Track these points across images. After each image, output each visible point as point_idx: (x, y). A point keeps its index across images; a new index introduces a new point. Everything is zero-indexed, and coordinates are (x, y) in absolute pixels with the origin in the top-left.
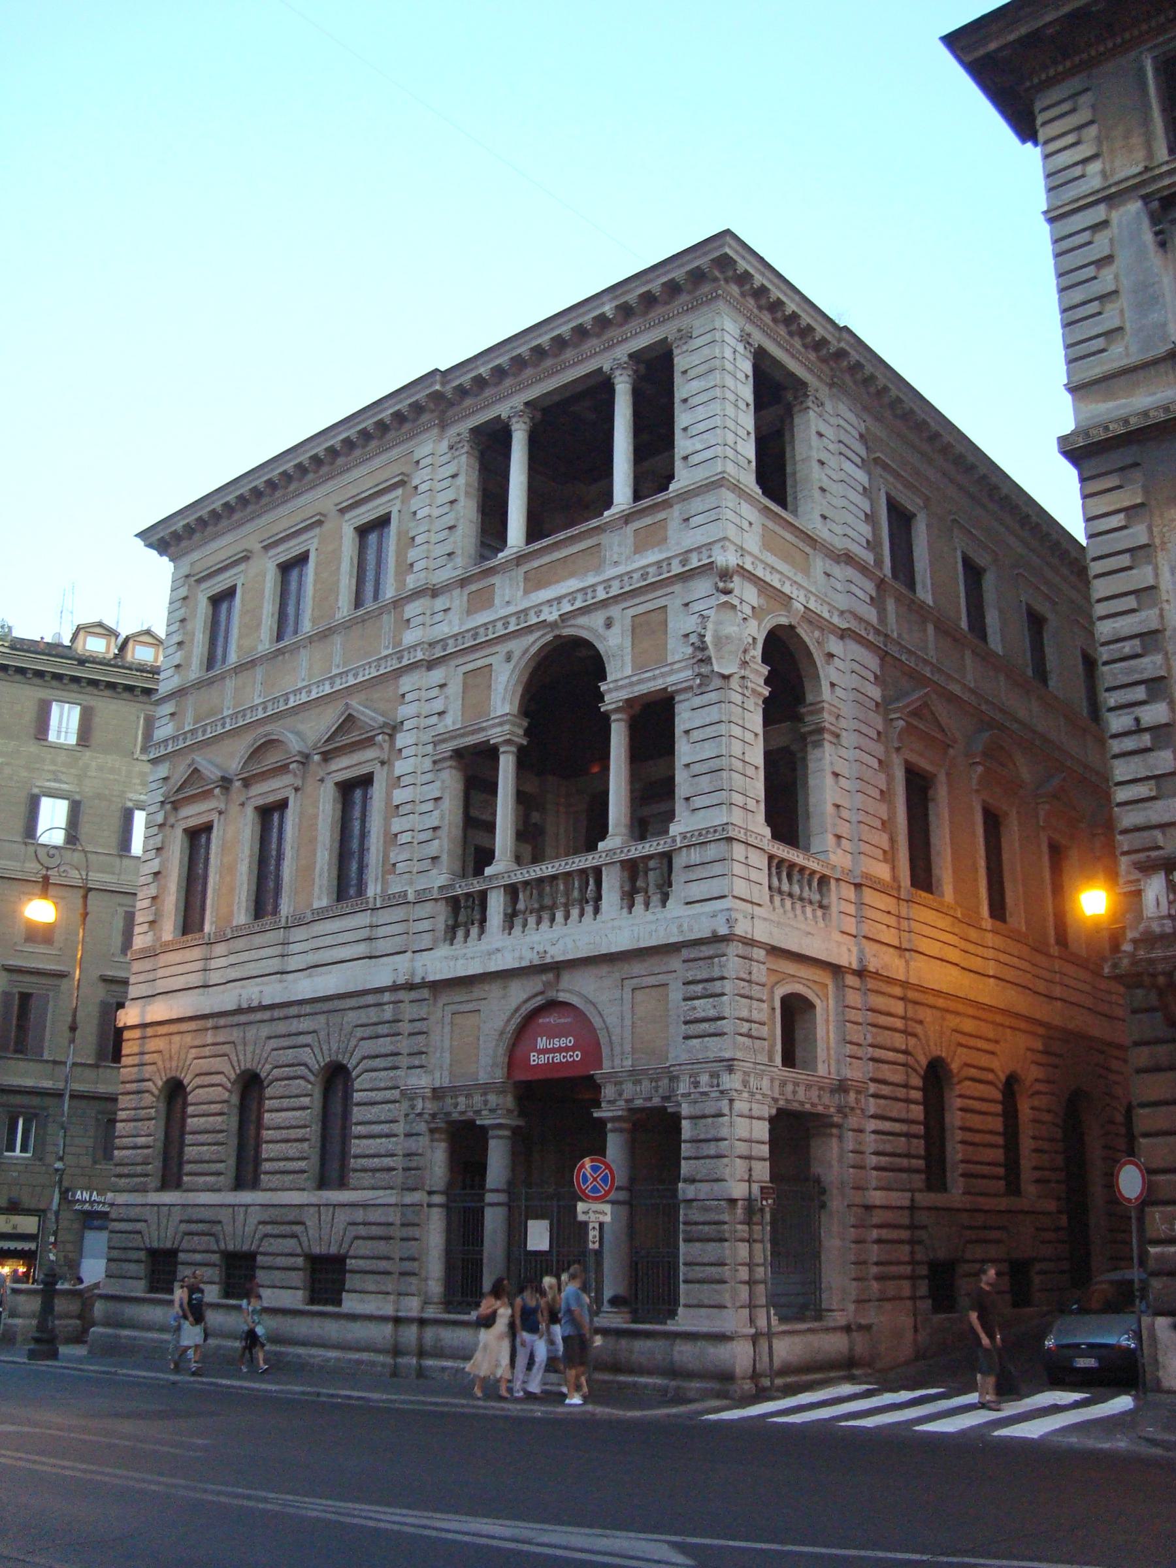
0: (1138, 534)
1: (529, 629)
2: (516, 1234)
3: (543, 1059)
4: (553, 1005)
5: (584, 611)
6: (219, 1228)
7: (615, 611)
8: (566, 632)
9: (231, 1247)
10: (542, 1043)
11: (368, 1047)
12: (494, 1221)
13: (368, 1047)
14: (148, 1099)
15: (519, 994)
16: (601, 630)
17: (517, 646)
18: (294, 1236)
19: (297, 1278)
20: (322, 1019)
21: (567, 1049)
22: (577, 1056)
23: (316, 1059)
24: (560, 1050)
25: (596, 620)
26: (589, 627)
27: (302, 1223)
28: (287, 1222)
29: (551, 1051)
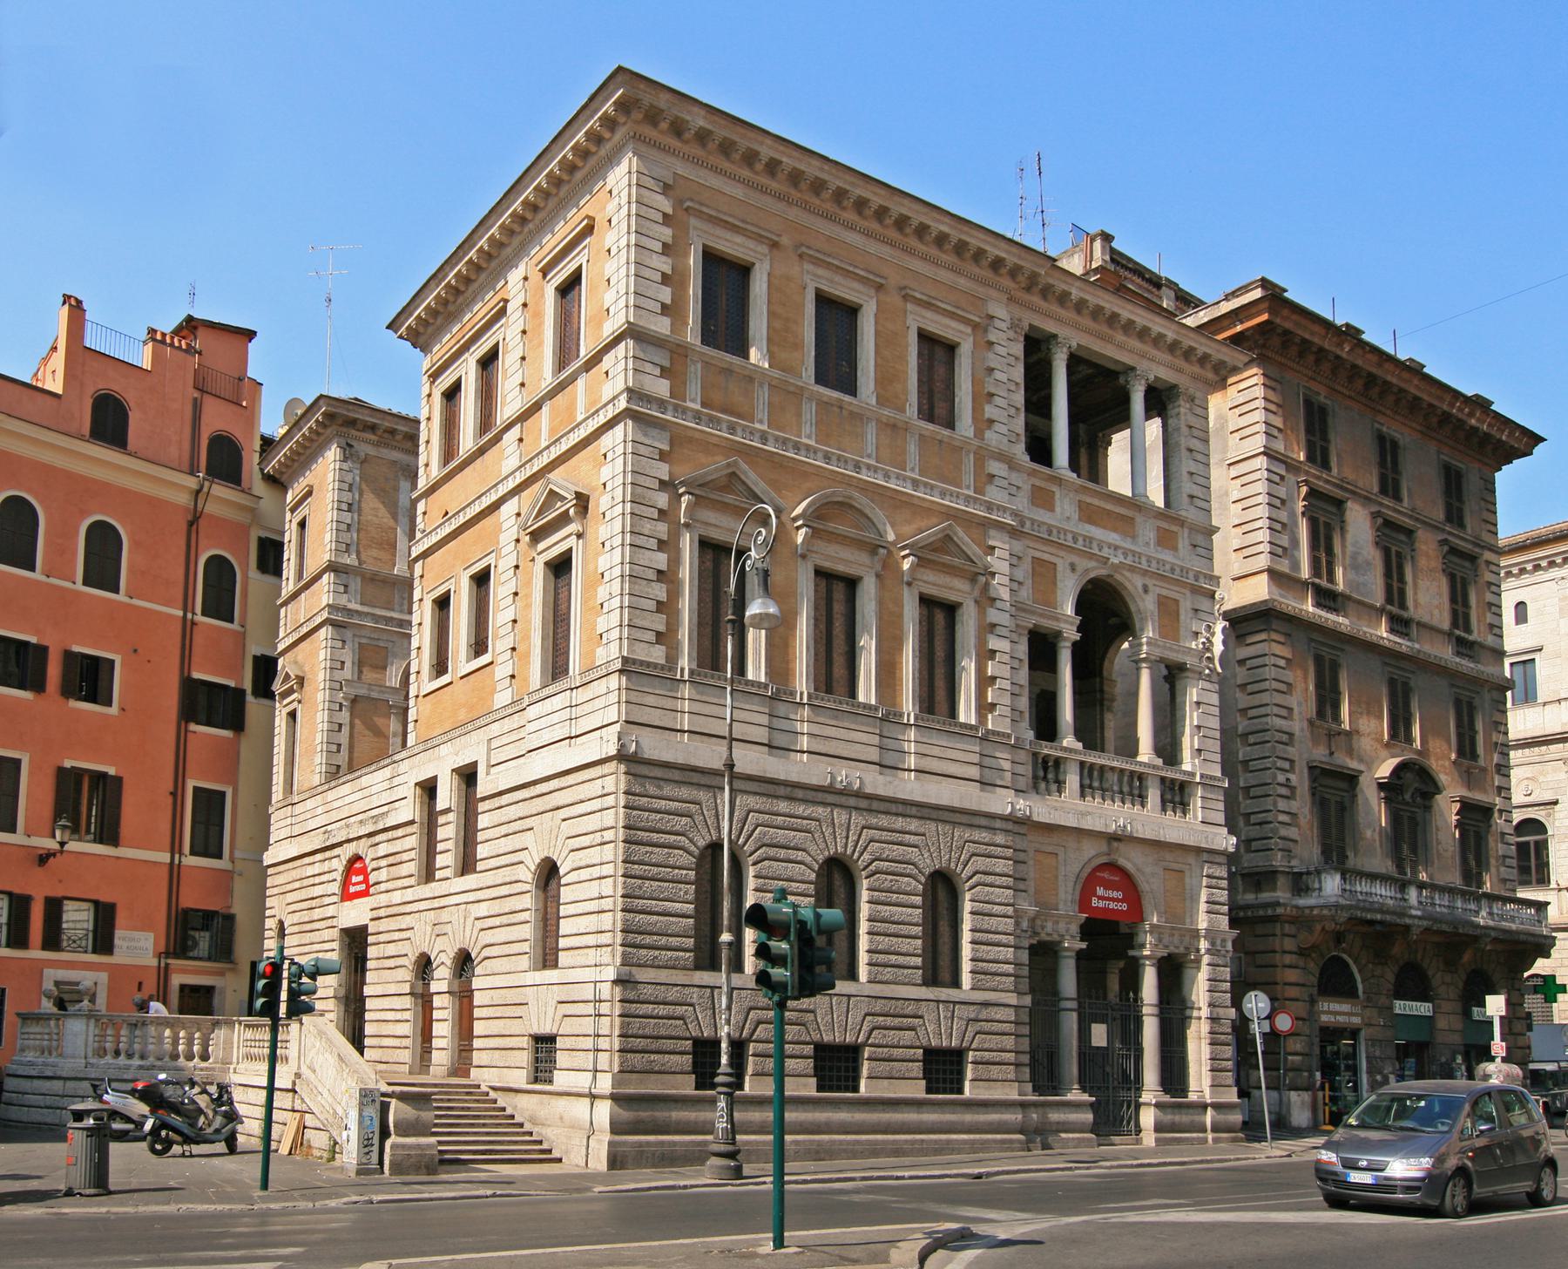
0: (1289, 676)
1: (1092, 556)
2: (1084, 1034)
3: (1101, 904)
4: (1112, 867)
5: (1132, 569)
6: (810, 1016)
7: (1150, 582)
8: (1118, 577)
9: (827, 1038)
10: (1100, 891)
11: (980, 863)
12: (1070, 1022)
13: (980, 863)
14: (751, 860)
15: (1090, 852)
16: (1140, 589)
17: (1083, 564)
18: (912, 1029)
19: (917, 1068)
20: (933, 826)
21: (1117, 900)
22: (1124, 907)
23: (928, 864)
24: (1113, 900)
25: (1138, 581)
26: (1132, 584)
27: (921, 1017)
28: (900, 1015)
29: (1107, 900)
